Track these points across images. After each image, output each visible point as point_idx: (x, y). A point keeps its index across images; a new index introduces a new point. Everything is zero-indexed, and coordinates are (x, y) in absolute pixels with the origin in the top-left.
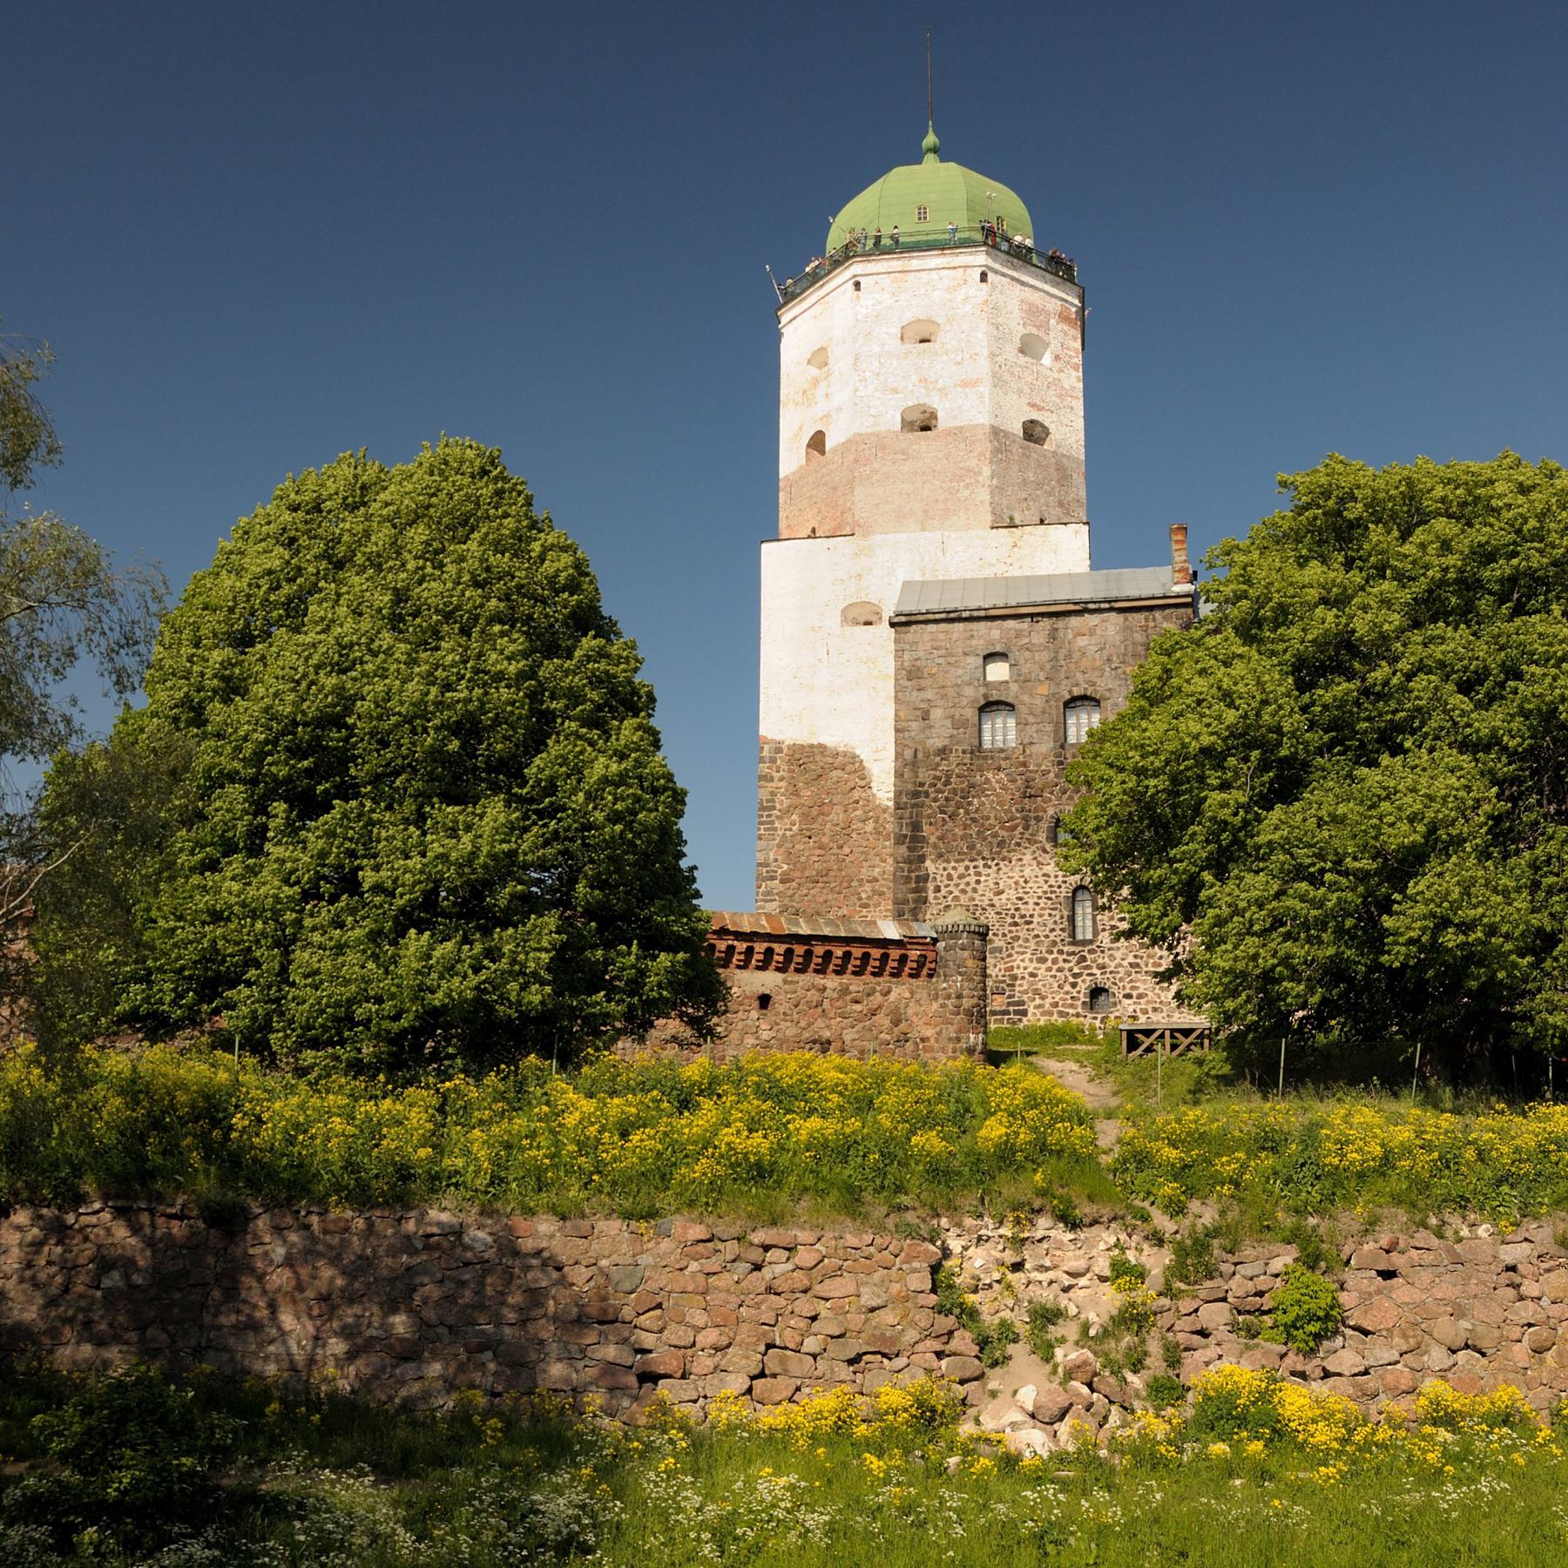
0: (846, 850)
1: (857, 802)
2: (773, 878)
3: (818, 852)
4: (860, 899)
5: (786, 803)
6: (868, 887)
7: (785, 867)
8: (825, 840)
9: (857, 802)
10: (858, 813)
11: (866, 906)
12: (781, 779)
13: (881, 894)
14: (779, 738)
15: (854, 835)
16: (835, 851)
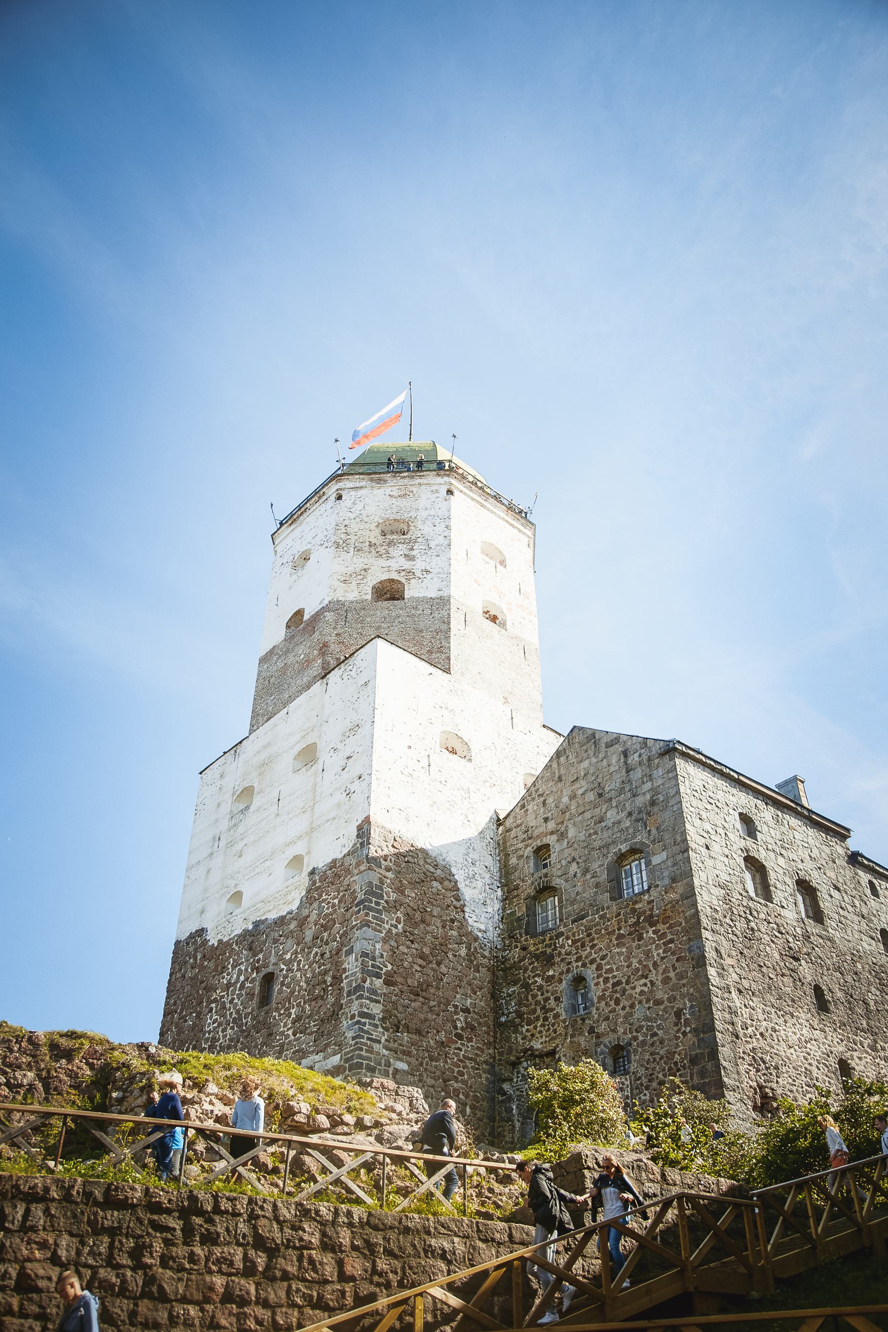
0: (443, 969)
1: (452, 921)
2: (378, 976)
3: (420, 961)
4: (456, 1028)
5: (393, 896)
6: (461, 1016)
7: (390, 967)
8: (426, 950)
9: (452, 921)
10: (455, 933)
11: (459, 1037)
12: (388, 869)
13: (473, 1028)
14: (389, 826)
15: (450, 955)
16: (435, 966)
